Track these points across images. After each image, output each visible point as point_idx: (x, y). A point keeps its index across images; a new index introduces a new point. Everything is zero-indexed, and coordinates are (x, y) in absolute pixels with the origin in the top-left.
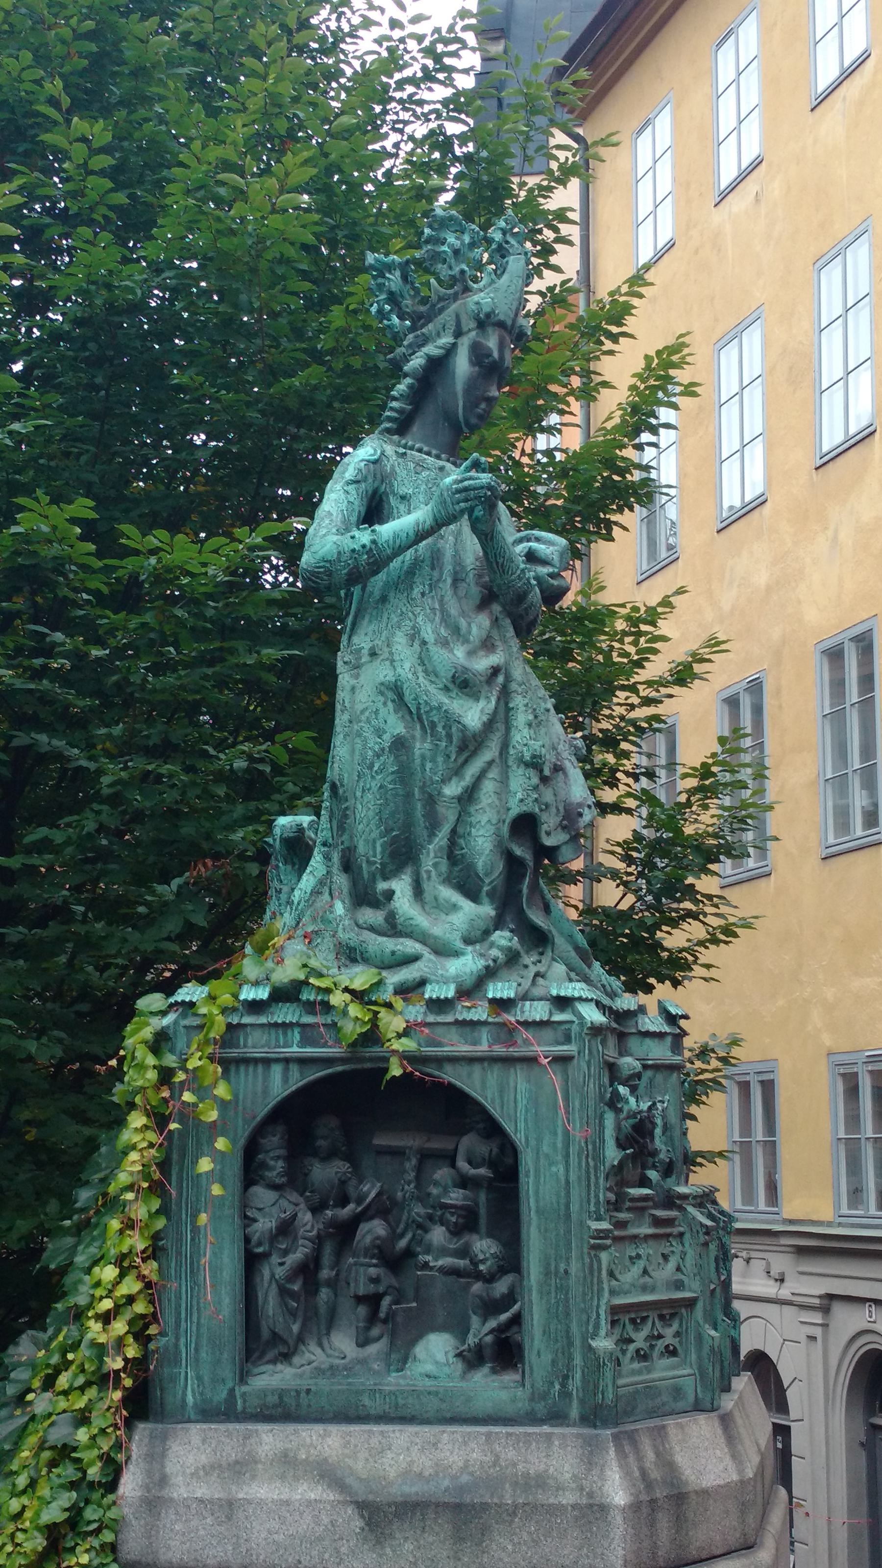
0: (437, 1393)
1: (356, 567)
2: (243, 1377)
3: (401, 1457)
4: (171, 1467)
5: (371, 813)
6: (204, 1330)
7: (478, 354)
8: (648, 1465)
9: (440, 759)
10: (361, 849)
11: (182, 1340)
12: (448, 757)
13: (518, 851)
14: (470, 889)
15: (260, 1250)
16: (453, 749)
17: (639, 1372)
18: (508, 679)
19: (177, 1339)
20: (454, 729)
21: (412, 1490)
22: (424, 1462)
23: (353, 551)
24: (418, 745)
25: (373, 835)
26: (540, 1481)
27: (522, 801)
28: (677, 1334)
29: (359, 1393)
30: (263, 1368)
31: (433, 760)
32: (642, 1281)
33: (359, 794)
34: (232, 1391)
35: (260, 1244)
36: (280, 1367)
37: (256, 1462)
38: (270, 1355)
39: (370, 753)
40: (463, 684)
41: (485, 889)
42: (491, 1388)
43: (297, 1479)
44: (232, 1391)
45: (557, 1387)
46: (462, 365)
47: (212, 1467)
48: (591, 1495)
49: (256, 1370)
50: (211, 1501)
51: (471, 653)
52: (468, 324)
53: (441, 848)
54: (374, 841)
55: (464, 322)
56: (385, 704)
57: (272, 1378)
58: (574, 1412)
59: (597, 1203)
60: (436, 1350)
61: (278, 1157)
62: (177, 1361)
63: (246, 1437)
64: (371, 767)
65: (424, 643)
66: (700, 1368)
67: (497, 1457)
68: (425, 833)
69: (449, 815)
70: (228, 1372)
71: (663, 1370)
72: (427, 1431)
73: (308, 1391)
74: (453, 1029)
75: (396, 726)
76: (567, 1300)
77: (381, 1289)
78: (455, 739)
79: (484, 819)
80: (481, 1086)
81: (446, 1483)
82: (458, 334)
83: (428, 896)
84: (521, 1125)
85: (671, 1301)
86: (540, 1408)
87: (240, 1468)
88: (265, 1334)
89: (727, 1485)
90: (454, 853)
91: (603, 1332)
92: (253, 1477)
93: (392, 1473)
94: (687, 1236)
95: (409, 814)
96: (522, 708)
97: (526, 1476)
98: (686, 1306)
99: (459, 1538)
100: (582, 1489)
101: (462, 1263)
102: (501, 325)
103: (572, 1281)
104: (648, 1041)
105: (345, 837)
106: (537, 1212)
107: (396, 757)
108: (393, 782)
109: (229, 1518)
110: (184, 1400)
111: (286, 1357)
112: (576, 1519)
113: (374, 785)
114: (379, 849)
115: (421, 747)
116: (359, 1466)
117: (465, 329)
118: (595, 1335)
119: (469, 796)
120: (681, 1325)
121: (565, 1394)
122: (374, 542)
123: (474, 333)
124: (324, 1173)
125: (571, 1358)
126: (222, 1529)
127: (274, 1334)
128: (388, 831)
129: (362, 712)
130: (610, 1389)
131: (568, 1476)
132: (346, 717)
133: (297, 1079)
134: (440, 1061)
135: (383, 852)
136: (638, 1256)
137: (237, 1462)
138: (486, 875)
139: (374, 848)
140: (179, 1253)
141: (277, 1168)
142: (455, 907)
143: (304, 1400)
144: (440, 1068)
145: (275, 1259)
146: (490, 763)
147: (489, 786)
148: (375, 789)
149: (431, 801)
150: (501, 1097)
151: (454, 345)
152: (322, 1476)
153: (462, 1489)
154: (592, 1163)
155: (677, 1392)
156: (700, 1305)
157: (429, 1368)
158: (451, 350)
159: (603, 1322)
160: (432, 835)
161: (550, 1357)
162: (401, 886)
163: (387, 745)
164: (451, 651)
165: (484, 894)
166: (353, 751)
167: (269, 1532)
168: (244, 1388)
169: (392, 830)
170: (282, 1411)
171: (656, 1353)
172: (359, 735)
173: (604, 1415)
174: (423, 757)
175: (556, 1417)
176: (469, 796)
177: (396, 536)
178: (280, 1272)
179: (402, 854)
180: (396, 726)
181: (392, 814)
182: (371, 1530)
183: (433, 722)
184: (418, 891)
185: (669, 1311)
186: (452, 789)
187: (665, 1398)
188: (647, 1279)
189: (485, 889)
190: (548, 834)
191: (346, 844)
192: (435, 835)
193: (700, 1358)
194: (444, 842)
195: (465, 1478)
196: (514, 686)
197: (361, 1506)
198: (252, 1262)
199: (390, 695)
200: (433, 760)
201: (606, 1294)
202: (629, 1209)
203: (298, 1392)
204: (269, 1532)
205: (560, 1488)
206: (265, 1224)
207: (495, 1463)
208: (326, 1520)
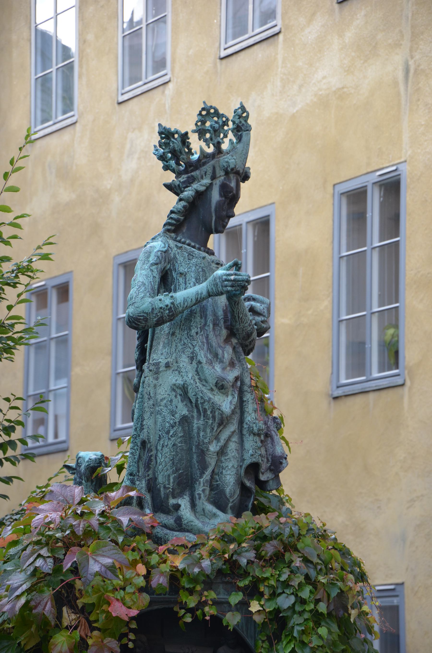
1: (162, 317)
5: (167, 460)
9: (208, 430)
10: (160, 479)
12: (213, 429)
13: (248, 484)
16: (216, 425)
18: (242, 383)
20: (217, 413)
23: (161, 308)
24: (195, 421)
25: (168, 472)
27: (252, 455)
31: (204, 431)
33: (159, 448)
39: (167, 425)
41: (230, 505)
46: (215, 196)
52: (220, 173)
53: (207, 481)
54: (169, 476)
56: (176, 396)
64: (168, 432)
65: (200, 362)
68: (198, 472)
69: (212, 461)
75: (182, 410)
79: (230, 465)
82: (213, 177)
83: (199, 508)
95: (190, 461)
96: (251, 401)
105: (150, 472)
107: (183, 428)
108: (181, 442)
113: (170, 443)
114: (172, 480)
115: (197, 423)
117: (218, 175)
119: (222, 452)
122: (172, 303)
128: (177, 470)
129: (162, 400)
132: (151, 402)
135: (174, 482)
138: (231, 497)
139: (169, 480)
146: (233, 433)
147: (233, 446)
149: (202, 453)
158: (209, 187)
160: (202, 473)
162: (184, 503)
163: (177, 420)
165: (229, 507)
166: (155, 423)
169: (180, 469)
172: (159, 413)
174: (199, 428)
176: (222, 452)
177: (185, 300)
179: (185, 483)
180: (182, 410)
181: (180, 460)
184: (193, 505)
186: (214, 448)
189: (230, 505)
191: (151, 476)
192: (204, 473)
194: (208, 478)
196: (246, 388)
199: (179, 391)
200: (204, 431)
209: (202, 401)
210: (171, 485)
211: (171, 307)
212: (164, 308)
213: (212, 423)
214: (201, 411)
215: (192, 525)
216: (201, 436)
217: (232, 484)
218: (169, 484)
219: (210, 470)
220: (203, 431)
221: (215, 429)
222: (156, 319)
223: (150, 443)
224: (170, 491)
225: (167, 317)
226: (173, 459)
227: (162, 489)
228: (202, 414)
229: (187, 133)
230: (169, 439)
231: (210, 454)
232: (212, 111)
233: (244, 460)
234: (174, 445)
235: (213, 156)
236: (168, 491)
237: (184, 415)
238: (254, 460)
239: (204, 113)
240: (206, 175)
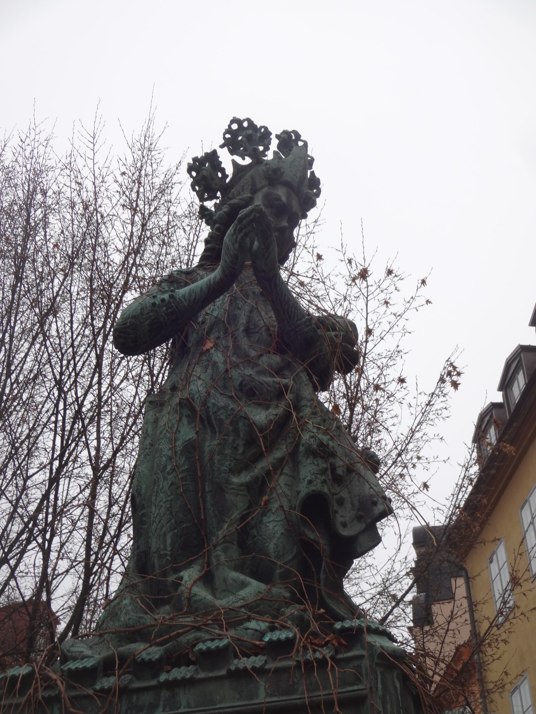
5: (163, 510)
7: (270, 201)
9: (228, 451)
12: (236, 448)
14: (262, 573)
16: (241, 442)
20: (241, 424)
27: (310, 482)
39: (164, 459)
40: (250, 392)
41: (278, 571)
54: (165, 535)
75: (187, 433)
78: (242, 434)
83: (218, 582)
90: (246, 539)
113: (166, 485)
114: (169, 541)
115: (210, 444)
117: (259, 186)
119: (258, 489)
122: (171, 297)
123: (265, 189)
138: (278, 557)
139: (165, 540)
142: (243, 585)
148: (166, 488)
163: (178, 449)
180: (187, 433)
183: (221, 420)
190: (344, 525)
199: (186, 412)
209: (216, 409)
210: (169, 549)
211: (169, 303)
212: (159, 305)
213: (234, 440)
214: (216, 426)
215: (195, 600)
216: (216, 461)
217: (278, 535)
218: (165, 549)
219: (235, 515)
220: (218, 455)
221: (241, 450)
222: (147, 322)
223: (141, 495)
224: (167, 559)
225: (166, 318)
226: (170, 507)
227: (156, 561)
228: (217, 429)
229: (214, 152)
230: (165, 478)
231: (233, 489)
232: (245, 124)
233: (298, 493)
234: (172, 484)
236: (164, 561)
237: (190, 439)
238: (313, 488)
239: (235, 126)
240: (243, 190)
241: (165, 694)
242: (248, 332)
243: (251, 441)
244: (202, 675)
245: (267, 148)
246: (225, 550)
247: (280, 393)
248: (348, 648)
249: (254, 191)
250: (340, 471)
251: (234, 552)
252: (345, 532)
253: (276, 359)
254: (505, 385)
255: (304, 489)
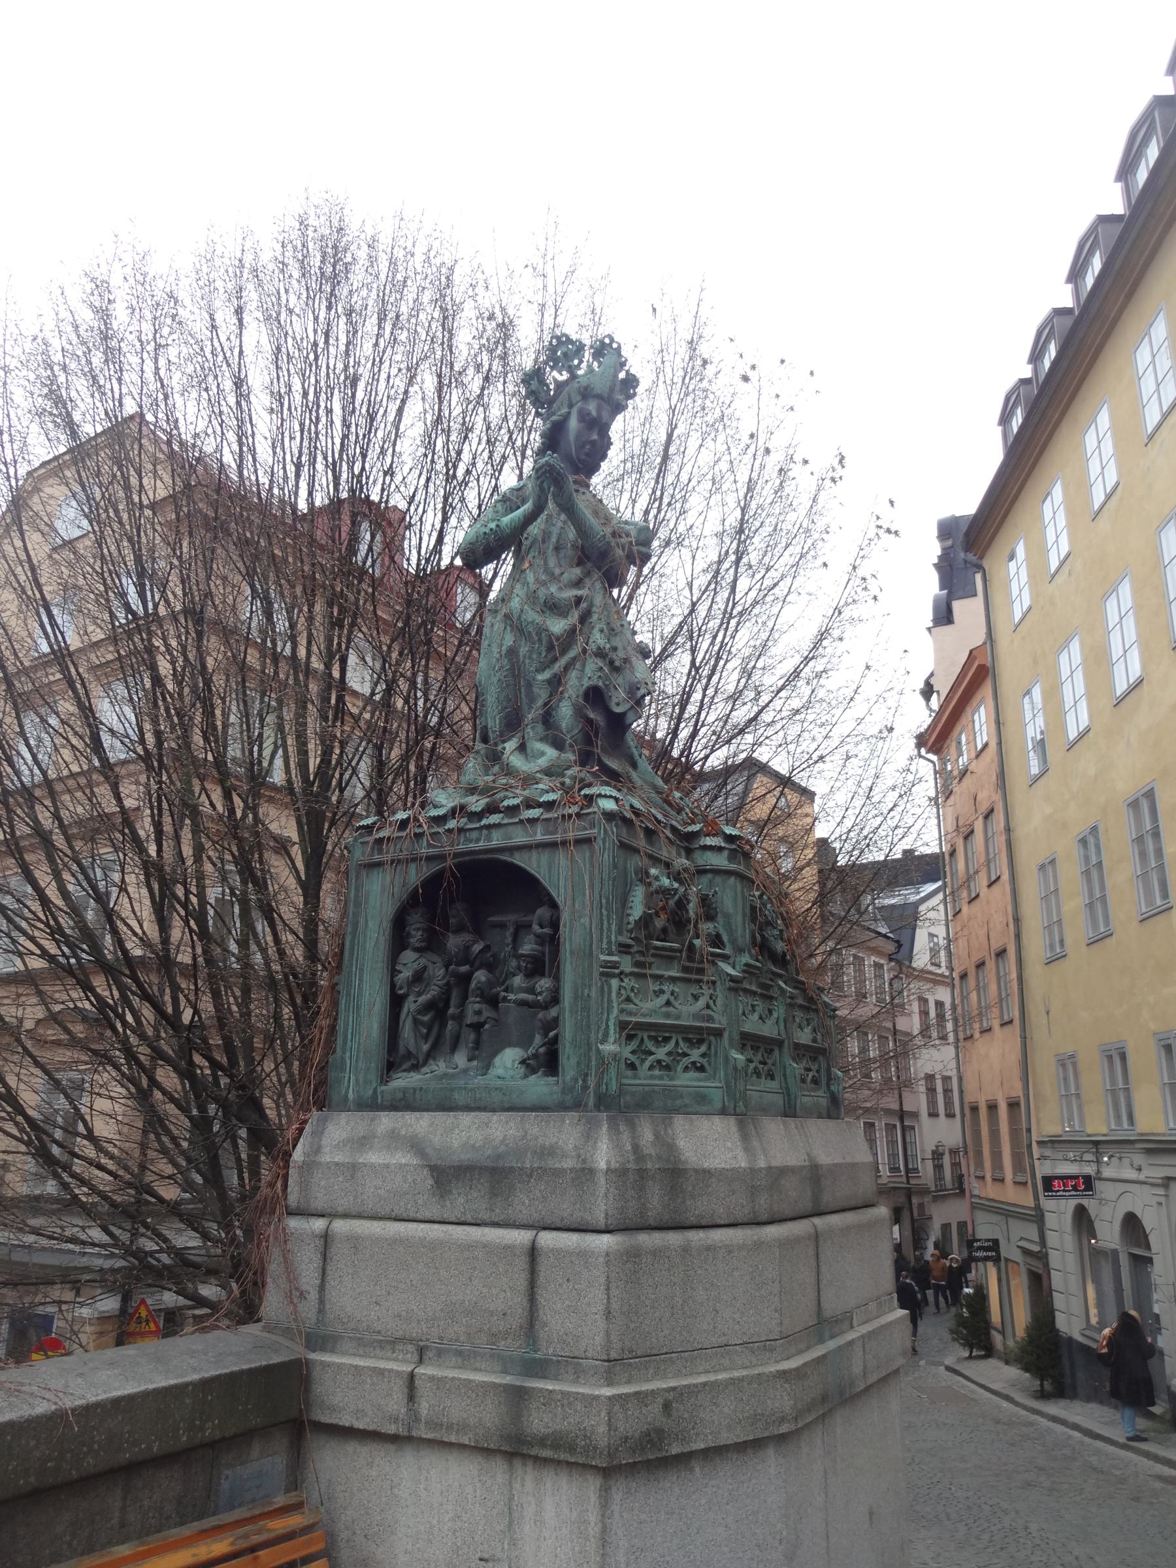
0: (501, 1089)
1: (488, 544)
2: (384, 1080)
3: (464, 1134)
4: (325, 1141)
6: (362, 1047)
7: (584, 417)
8: (642, 1143)
9: (535, 656)
11: (348, 1054)
14: (558, 745)
15: (401, 992)
16: (543, 649)
17: (661, 1078)
18: (591, 605)
19: (344, 1053)
21: (466, 1157)
22: (477, 1137)
26: (551, 1151)
28: (703, 1055)
29: (452, 1090)
30: (400, 1075)
31: (530, 658)
32: (664, 1009)
34: (375, 1089)
35: (401, 988)
36: (412, 1074)
37: (374, 1137)
38: (405, 1066)
40: (553, 607)
42: (539, 1086)
43: (396, 1149)
44: (375, 1089)
45: (580, 1082)
47: (348, 1141)
48: (584, 1161)
49: (395, 1076)
50: (343, 1164)
51: (560, 589)
52: (576, 398)
55: (573, 395)
57: (403, 1081)
58: (591, 1102)
59: (609, 942)
60: (509, 1059)
61: (418, 929)
62: (343, 1070)
63: (372, 1120)
66: (727, 1084)
67: (526, 1133)
70: (373, 1077)
71: (686, 1080)
72: (484, 1115)
73: (421, 1089)
74: (519, 826)
76: (588, 1016)
77: (482, 1020)
80: (535, 864)
81: (489, 1152)
83: (529, 750)
84: (562, 891)
85: (701, 1028)
86: (568, 1098)
87: (363, 1142)
88: (402, 1051)
89: (733, 1169)
90: (547, 719)
91: (612, 1040)
92: (371, 1147)
93: (456, 1144)
94: (718, 983)
97: (543, 1147)
98: (715, 1035)
99: (493, 1194)
100: (579, 1156)
101: (530, 997)
102: (599, 397)
103: (592, 1003)
104: (709, 854)
106: (572, 952)
109: (352, 1177)
110: (346, 1096)
111: (416, 1067)
112: (573, 1180)
113: (495, 680)
115: (523, 650)
116: (436, 1140)
118: (604, 1040)
120: (709, 1048)
121: (585, 1087)
122: (498, 526)
124: (454, 942)
125: (590, 1060)
126: (348, 1185)
127: (409, 1053)
130: (614, 1082)
131: (571, 1146)
132: (487, 643)
133: (427, 871)
134: (511, 849)
136: (662, 992)
137: (363, 1137)
140: (348, 994)
141: (416, 936)
142: (543, 754)
143: (418, 1096)
144: (511, 856)
145: (411, 998)
146: (574, 659)
149: (529, 685)
150: (550, 871)
151: (569, 413)
152: (412, 1147)
153: (499, 1157)
154: (605, 912)
155: (702, 1099)
156: (726, 1034)
157: (500, 1072)
159: (612, 1032)
161: (576, 1059)
164: (548, 589)
167: (376, 1188)
168: (383, 1088)
170: (404, 1103)
171: (680, 1068)
173: (615, 1105)
174: (524, 657)
175: (578, 1105)
178: (413, 1007)
179: (513, 723)
182: (438, 1187)
185: (697, 1036)
187: (687, 1101)
188: (671, 1009)
190: (618, 704)
193: (726, 1075)
195: (502, 1148)
196: (594, 609)
197: (433, 1169)
198: (396, 1002)
201: (615, 1011)
202: (653, 955)
203: (415, 1090)
204: (376, 1188)
205: (564, 1156)
206: (406, 974)
207: (524, 1137)
208: (410, 1180)
219: (540, 703)
235: (566, 383)
241: (485, 832)
242: (557, 549)
243: (551, 648)
244: (506, 821)
245: (581, 362)
246: (533, 728)
247: (579, 600)
248: (589, 806)
249: (571, 406)
250: (617, 663)
251: (540, 728)
252: (618, 710)
253: (577, 571)
254: (1035, 357)
255: (586, 683)
